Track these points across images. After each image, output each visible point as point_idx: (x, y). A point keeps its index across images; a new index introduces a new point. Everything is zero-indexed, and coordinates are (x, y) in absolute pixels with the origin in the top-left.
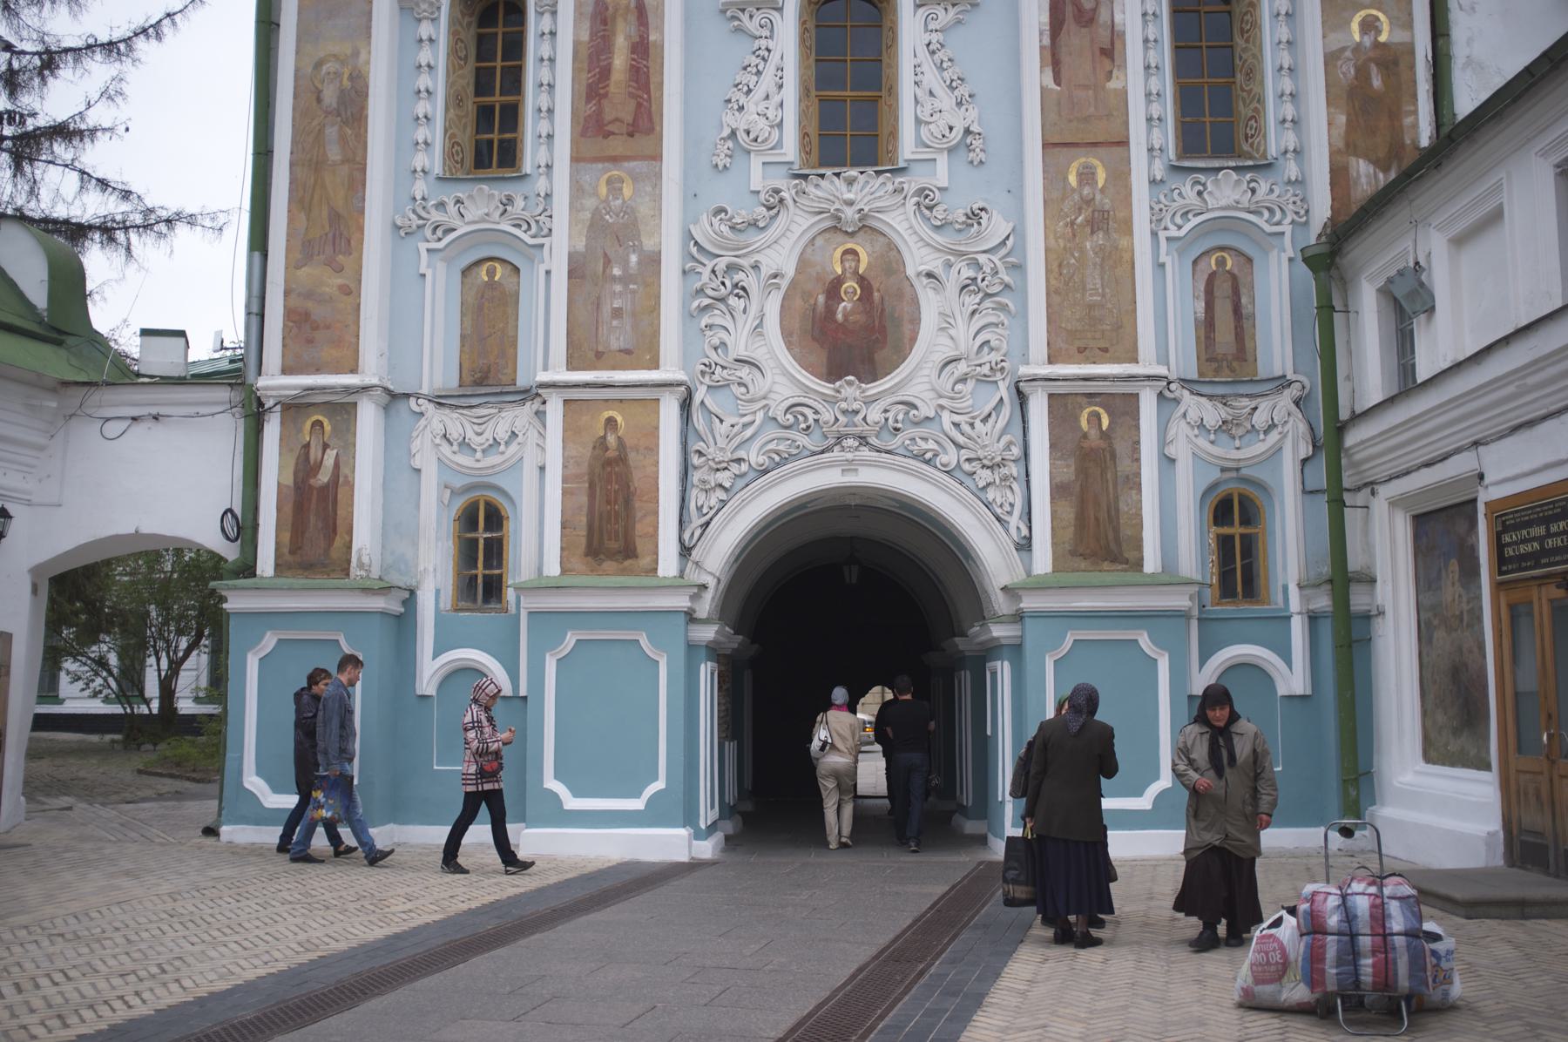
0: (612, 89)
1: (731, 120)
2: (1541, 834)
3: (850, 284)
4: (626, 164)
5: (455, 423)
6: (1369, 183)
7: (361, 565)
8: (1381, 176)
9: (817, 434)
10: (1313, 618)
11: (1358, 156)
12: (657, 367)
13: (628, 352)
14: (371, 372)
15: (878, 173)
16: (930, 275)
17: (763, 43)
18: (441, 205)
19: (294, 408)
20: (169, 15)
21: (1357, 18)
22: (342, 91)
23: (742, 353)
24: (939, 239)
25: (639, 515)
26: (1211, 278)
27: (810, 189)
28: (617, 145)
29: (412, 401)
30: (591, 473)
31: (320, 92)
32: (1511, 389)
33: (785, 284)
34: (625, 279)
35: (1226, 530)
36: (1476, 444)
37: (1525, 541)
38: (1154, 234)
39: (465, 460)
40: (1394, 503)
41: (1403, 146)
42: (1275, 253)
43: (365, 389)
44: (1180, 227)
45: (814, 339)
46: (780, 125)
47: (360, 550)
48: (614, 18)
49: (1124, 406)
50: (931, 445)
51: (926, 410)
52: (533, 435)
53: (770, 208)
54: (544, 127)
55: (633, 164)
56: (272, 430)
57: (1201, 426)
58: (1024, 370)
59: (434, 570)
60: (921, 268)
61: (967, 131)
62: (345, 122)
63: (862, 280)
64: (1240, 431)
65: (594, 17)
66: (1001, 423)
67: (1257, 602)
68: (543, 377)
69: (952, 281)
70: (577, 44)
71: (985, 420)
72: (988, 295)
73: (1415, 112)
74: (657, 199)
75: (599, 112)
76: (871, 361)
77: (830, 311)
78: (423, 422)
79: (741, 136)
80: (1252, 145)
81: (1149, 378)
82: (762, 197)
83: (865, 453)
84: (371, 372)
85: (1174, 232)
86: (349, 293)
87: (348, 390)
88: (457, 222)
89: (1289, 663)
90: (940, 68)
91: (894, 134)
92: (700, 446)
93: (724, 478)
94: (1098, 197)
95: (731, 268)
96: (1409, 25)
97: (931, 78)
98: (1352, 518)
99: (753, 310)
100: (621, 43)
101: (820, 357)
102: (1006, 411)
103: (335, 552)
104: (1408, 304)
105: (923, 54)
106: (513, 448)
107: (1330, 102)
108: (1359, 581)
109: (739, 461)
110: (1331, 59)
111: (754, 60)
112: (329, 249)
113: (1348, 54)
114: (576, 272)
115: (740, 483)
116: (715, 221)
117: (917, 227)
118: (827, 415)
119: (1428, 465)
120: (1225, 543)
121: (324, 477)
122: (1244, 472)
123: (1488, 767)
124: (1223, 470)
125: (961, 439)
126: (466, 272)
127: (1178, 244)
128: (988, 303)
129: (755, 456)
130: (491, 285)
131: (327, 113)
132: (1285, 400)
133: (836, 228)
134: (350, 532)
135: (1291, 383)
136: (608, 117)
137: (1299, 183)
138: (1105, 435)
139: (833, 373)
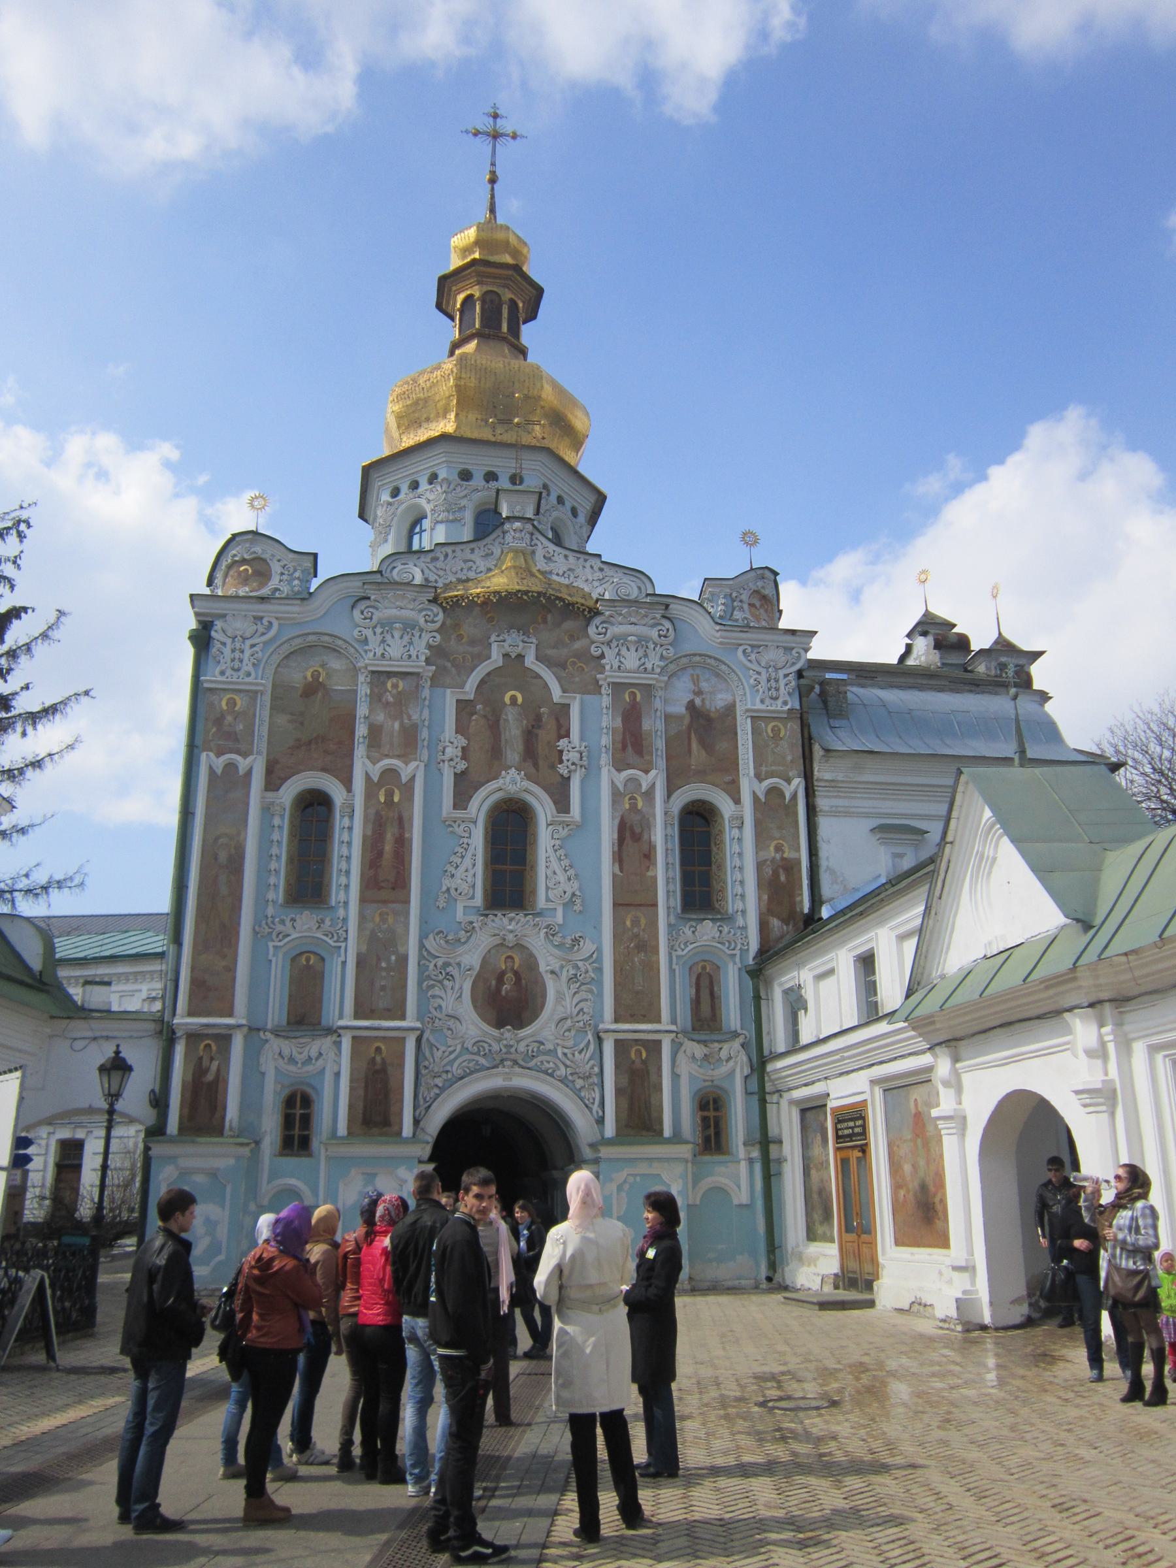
1: (447, 883)
2: (855, 1272)
3: (510, 975)
5: (287, 1046)
7: (231, 1129)
13: (389, 1010)
15: (526, 915)
16: (552, 972)
17: (466, 840)
18: (283, 922)
19: (194, 1037)
20: (50, 755)
21: (773, 844)
23: (451, 1012)
29: (261, 1033)
32: (838, 1057)
36: (826, 1078)
38: (670, 954)
39: (292, 1068)
43: (239, 1026)
47: (231, 1121)
51: (550, 1046)
52: (332, 1055)
55: (394, 905)
56: (180, 1050)
57: (693, 1057)
58: (601, 1026)
63: (516, 973)
66: (588, 1055)
68: (341, 1023)
69: (564, 976)
70: (364, 836)
71: (580, 1052)
72: (583, 984)
73: (801, 895)
77: (498, 990)
78: (267, 1046)
79: (453, 892)
81: (667, 1031)
83: (517, 1069)
84: (240, 1016)
85: (680, 953)
86: (230, 970)
88: (291, 931)
89: (739, 1187)
90: (560, 860)
91: (534, 892)
92: (427, 1063)
95: (446, 964)
96: (798, 849)
97: (555, 865)
98: (771, 1109)
99: (457, 987)
100: (389, 837)
102: (592, 1047)
104: (796, 1003)
106: (320, 1062)
108: (774, 1142)
109: (447, 1072)
110: (760, 866)
114: (361, 963)
116: (437, 938)
118: (496, 1047)
119: (806, 1085)
120: (705, 1120)
121: (210, 1077)
123: (832, 1241)
125: (568, 1063)
126: (293, 960)
128: (583, 987)
129: (456, 1070)
130: (308, 967)
132: (736, 1044)
134: (225, 1108)
137: (745, 928)
138: (644, 1062)
139: (499, 1024)
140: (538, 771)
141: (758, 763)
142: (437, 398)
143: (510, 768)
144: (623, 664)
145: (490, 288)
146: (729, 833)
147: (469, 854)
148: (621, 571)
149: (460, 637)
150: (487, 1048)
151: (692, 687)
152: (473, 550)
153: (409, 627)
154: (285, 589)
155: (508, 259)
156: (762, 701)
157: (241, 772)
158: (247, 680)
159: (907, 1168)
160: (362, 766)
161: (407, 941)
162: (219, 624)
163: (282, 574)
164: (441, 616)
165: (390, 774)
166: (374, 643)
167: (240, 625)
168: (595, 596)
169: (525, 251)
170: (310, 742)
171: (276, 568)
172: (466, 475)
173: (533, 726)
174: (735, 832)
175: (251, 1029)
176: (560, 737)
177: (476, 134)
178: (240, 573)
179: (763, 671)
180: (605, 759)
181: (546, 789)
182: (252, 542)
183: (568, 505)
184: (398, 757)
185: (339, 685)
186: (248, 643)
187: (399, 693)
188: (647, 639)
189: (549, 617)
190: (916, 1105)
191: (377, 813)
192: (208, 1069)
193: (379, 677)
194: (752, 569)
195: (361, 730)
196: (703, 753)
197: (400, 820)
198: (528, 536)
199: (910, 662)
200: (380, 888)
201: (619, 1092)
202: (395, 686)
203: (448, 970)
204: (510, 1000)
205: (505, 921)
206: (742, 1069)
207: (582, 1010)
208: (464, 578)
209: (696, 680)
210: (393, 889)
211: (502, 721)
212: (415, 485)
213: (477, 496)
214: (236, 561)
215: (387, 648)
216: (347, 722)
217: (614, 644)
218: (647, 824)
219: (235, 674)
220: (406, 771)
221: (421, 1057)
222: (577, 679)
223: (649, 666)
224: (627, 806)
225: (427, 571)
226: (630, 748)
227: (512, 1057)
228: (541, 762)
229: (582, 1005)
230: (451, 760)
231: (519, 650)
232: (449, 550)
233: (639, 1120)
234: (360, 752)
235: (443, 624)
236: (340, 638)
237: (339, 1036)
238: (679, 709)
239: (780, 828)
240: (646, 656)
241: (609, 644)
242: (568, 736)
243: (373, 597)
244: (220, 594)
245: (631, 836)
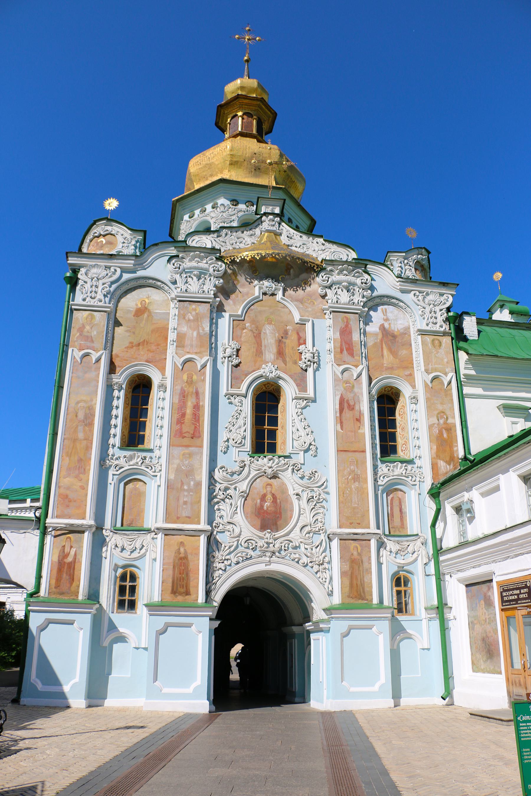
0: (186, 421)
3: (269, 497)
4: (190, 448)
6: (444, 469)
8: (448, 466)
11: (440, 459)
12: (199, 524)
13: (189, 517)
15: (280, 457)
16: (297, 495)
17: (240, 408)
25: (192, 579)
28: (186, 441)
30: (174, 562)
31: (77, 413)
35: (399, 589)
40: (459, 581)
41: (454, 457)
44: (383, 481)
45: (256, 515)
46: (245, 438)
48: (187, 396)
62: (86, 425)
64: (404, 553)
65: (180, 394)
67: (413, 614)
69: (305, 496)
71: (316, 548)
73: (457, 446)
75: (181, 429)
76: (276, 524)
77: (262, 506)
79: (231, 441)
80: (404, 453)
86: (84, 489)
89: (422, 637)
94: (356, 470)
95: (226, 489)
96: (454, 417)
100: (190, 404)
101: (258, 522)
103: (73, 589)
105: (295, 416)
107: (431, 441)
109: (227, 560)
110: (430, 427)
112: (77, 472)
113: (436, 425)
114: (169, 487)
117: (295, 479)
120: (399, 593)
131: (80, 421)
136: (184, 431)
139: (263, 528)
140: (286, 365)
142: (217, 163)
143: (268, 362)
156: (427, 325)
158: (100, 304)
161: (201, 471)
162: (83, 270)
163: (124, 243)
168: (320, 259)
170: (139, 345)
173: (282, 337)
176: (300, 344)
178: (97, 243)
181: (291, 376)
184: (196, 353)
186: (101, 282)
187: (197, 314)
188: (354, 284)
189: (292, 271)
192: (68, 554)
195: (172, 336)
196: (391, 357)
197: (197, 393)
198: (277, 225)
201: (343, 574)
205: (266, 460)
207: (317, 520)
211: (262, 333)
215: (189, 286)
216: (163, 332)
219: (93, 301)
222: (310, 309)
223: (356, 302)
225: (214, 243)
226: (345, 352)
228: (288, 359)
230: (230, 357)
234: (171, 350)
236: (159, 281)
239: (442, 404)
241: (330, 287)
242: (305, 343)
243: (180, 255)
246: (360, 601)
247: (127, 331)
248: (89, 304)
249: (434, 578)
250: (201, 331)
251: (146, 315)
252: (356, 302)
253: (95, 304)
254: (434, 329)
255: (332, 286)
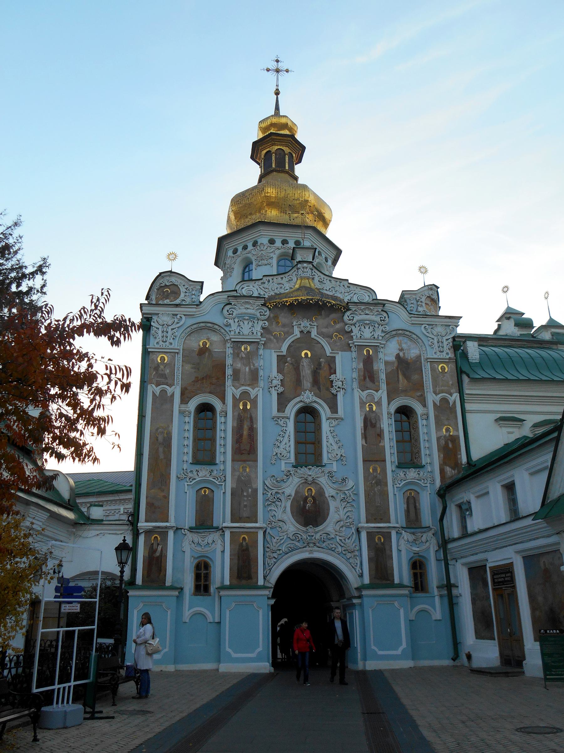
1: (276, 450)
5: (196, 537)
9: (301, 542)
10: (441, 596)
13: (248, 517)
14: (172, 522)
16: (332, 496)
19: (149, 532)
22: (164, 437)
23: (280, 519)
24: (335, 486)
26: (408, 499)
27: (298, 471)
29: (183, 530)
33: (292, 498)
34: (247, 496)
35: (415, 571)
37: (500, 578)
39: (199, 549)
40: (463, 564)
42: (425, 492)
46: (290, 452)
49: (388, 536)
50: (334, 546)
52: (219, 542)
53: (287, 476)
54: (222, 450)
56: (142, 539)
58: (360, 525)
59: (189, 583)
60: (330, 495)
61: (341, 455)
63: (313, 497)
66: (353, 540)
68: (224, 525)
71: (348, 539)
73: (461, 454)
74: (256, 473)
79: (279, 455)
82: (285, 472)
83: (315, 548)
84: (172, 522)
85: (398, 485)
87: (166, 527)
88: (196, 477)
89: (435, 611)
92: (268, 545)
93: (275, 555)
96: (457, 430)
97: (331, 440)
99: (283, 506)
102: (354, 536)
104: (465, 510)
105: (329, 433)
109: (280, 550)
110: (438, 439)
111: (282, 433)
113: (443, 438)
115: (280, 556)
118: (304, 537)
119: (473, 555)
120: (415, 575)
121: (158, 554)
122: (420, 554)
124: (414, 553)
125: (342, 545)
127: (399, 489)
128: (348, 505)
129: (284, 548)
132: (430, 534)
133: (306, 482)
135: (431, 529)
139: (306, 524)
140: (320, 392)
141: (435, 386)
142: (255, 203)
144: (364, 335)
145: (279, 147)
146: (421, 422)
147: (287, 436)
148: (359, 288)
149: (278, 323)
150: (300, 537)
151: (398, 347)
152: (282, 278)
153: (252, 318)
154: (188, 300)
155: (286, 132)
157: (169, 395)
158: (170, 347)
159: (540, 599)
160: (231, 391)
162: (155, 318)
164: (268, 313)
165: (245, 394)
166: (234, 327)
167: (166, 319)
168: (346, 301)
169: (295, 129)
171: (183, 289)
172: (272, 242)
174: (424, 422)
175: (177, 529)
177: (268, 70)
178: (164, 292)
179: (435, 338)
180: (355, 385)
182: (170, 276)
183: (323, 256)
185: (217, 349)
186: (170, 328)
190: (545, 565)
191: (239, 415)
193: (237, 344)
194: (425, 286)
196: (406, 381)
199: (501, 333)
200: (242, 454)
201: (370, 560)
202: (246, 349)
203: (278, 496)
204: (311, 512)
206: (434, 547)
208: (278, 293)
209: (400, 344)
210: (249, 454)
211: (301, 367)
212: (245, 247)
213: (278, 252)
214: (162, 287)
215: (241, 329)
216: (221, 367)
217: (357, 326)
218: (378, 418)
220: (253, 393)
221: (266, 543)
223: (376, 337)
224: (368, 409)
227: (313, 541)
228: (321, 387)
229: (348, 514)
230: (276, 386)
231: (308, 329)
232: (270, 278)
233: (382, 575)
235: (269, 317)
236: (216, 325)
237: (223, 532)
238: (392, 358)
239: (448, 419)
240: (374, 330)
241: (354, 324)
244: (154, 302)
245: (371, 424)
246: (384, 582)
247: (192, 368)
248: (161, 347)
249: (443, 562)
250: (252, 367)
251: (207, 354)
252: (376, 337)
253: (167, 347)
254: (442, 357)
255: (356, 323)
